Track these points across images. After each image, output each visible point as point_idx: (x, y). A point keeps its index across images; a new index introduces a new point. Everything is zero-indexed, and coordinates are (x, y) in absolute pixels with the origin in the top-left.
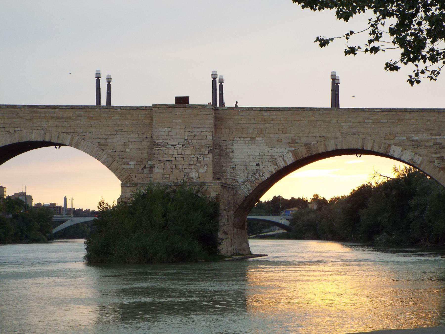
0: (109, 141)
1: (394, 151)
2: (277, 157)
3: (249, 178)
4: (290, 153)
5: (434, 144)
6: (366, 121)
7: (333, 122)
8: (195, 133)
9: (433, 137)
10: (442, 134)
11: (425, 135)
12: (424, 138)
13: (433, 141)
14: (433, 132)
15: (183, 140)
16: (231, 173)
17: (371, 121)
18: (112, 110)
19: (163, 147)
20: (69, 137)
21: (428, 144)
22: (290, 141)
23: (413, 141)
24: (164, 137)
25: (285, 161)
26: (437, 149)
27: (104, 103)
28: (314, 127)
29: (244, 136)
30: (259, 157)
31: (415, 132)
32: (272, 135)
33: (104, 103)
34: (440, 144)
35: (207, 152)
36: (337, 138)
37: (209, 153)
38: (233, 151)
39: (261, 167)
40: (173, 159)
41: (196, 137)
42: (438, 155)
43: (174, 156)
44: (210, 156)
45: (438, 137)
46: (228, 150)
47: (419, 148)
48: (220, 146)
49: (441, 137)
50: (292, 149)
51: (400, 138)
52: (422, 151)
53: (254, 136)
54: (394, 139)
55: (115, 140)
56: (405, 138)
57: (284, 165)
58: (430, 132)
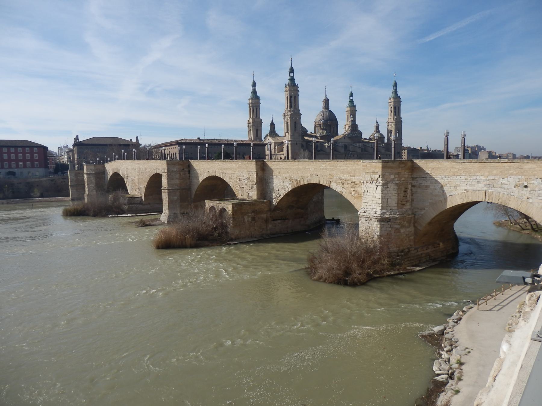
0: (232, 176)
1: (333, 186)
3: (276, 197)
4: (290, 185)
5: (352, 182)
6: (321, 167)
7: (306, 168)
8: (251, 174)
9: (351, 178)
10: (356, 176)
11: (347, 176)
15: (247, 178)
16: (270, 194)
17: (322, 167)
18: (233, 162)
19: (241, 180)
26: (353, 185)
28: (299, 171)
31: (343, 175)
32: (283, 175)
35: (254, 184)
37: (255, 184)
38: (270, 183)
39: (280, 191)
40: (244, 187)
43: (245, 185)
44: (256, 185)
45: (354, 178)
46: (268, 182)
47: (345, 184)
48: (266, 180)
50: (291, 182)
52: (346, 186)
56: (338, 178)
57: (288, 191)
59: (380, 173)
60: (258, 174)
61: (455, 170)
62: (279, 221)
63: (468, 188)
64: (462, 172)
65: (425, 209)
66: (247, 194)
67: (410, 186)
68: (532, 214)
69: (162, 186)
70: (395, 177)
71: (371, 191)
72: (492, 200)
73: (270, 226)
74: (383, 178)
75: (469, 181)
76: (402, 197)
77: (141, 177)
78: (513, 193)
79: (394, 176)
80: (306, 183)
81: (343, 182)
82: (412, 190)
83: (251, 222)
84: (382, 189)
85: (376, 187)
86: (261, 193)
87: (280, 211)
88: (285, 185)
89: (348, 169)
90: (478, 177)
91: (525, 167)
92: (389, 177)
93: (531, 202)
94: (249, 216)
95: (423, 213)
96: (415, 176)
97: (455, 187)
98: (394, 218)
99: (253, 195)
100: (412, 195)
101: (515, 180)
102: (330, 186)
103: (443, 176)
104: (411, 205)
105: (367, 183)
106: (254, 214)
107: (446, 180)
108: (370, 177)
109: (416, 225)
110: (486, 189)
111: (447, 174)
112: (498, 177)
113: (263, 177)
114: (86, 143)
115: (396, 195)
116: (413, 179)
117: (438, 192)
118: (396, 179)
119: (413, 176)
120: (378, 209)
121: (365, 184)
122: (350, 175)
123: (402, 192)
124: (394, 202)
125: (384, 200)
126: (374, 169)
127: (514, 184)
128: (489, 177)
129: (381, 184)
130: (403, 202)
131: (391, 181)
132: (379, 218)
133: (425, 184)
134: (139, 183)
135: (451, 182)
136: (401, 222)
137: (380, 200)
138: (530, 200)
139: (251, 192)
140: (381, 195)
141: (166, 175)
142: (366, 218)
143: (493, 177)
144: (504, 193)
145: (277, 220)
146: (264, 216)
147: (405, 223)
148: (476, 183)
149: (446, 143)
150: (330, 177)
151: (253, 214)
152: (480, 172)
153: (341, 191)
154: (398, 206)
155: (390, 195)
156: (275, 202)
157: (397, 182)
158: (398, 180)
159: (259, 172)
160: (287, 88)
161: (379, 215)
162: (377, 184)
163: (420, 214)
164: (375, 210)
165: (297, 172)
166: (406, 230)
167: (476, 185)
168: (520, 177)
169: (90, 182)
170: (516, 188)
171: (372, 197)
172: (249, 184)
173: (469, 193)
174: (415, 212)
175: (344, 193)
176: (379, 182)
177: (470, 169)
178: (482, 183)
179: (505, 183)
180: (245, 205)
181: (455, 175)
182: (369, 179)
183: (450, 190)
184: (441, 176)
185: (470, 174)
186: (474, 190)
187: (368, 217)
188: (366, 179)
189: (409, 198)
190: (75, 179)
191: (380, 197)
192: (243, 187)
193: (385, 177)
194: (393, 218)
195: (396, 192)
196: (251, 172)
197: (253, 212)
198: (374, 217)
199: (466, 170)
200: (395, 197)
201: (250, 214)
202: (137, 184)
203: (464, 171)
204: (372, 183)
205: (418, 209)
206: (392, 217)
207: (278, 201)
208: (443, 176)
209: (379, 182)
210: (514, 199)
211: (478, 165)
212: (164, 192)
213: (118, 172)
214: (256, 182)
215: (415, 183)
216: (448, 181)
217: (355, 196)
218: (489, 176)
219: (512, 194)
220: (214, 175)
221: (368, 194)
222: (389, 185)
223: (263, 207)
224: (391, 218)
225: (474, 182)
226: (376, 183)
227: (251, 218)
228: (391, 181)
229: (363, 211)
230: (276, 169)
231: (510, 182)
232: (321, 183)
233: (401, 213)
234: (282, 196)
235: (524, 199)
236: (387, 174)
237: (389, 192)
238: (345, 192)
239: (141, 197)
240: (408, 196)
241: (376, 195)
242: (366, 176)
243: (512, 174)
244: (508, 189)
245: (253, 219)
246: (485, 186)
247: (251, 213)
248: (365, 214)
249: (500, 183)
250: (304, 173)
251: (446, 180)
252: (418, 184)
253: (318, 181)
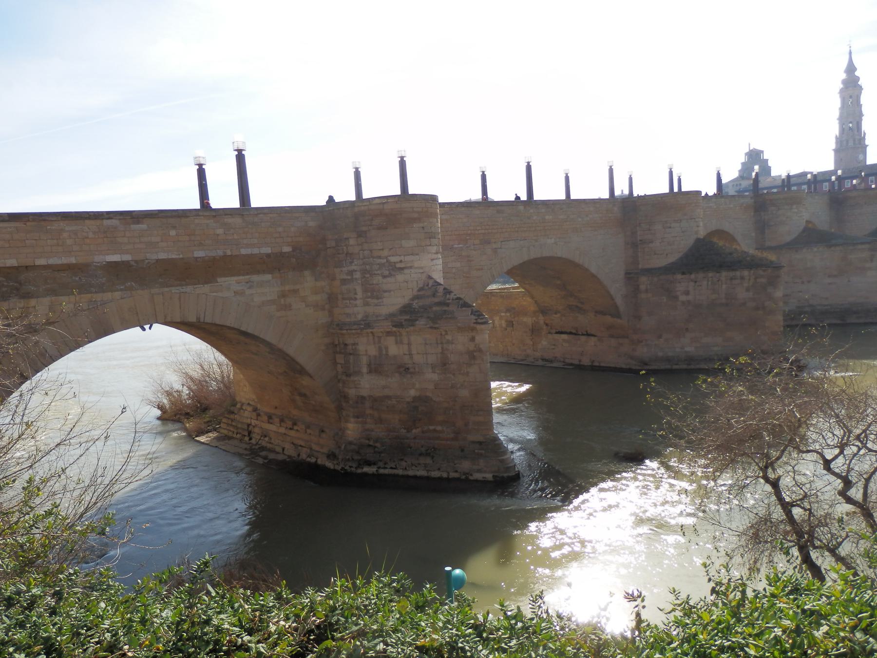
27: (676, 190)
33: (676, 190)
62: (564, 336)
73: (544, 343)
94: (501, 318)
106: (511, 315)
145: (562, 333)
146: (528, 320)
151: (508, 314)
180: (493, 296)
197: (508, 310)
201: (503, 314)
223: (525, 303)
227: (506, 321)
245: (510, 324)
247: (506, 312)
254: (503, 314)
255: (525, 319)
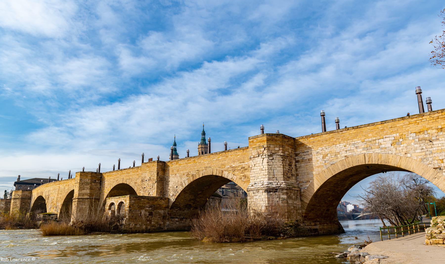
0: (137, 181)
1: (225, 174)
2: (183, 182)
5: (241, 168)
6: (214, 160)
7: (201, 162)
8: (152, 174)
9: (241, 164)
10: (245, 162)
11: (237, 163)
12: (237, 165)
13: (241, 166)
14: (241, 161)
15: (149, 178)
17: (216, 159)
20: (128, 180)
21: (239, 168)
22: (187, 174)
23: (233, 167)
24: (144, 177)
25: (185, 184)
26: (243, 171)
28: (195, 166)
29: (173, 173)
30: (177, 183)
32: (181, 172)
34: (244, 168)
35: (155, 183)
36: (203, 170)
38: (169, 181)
39: (178, 188)
40: (146, 187)
41: (152, 176)
42: (243, 174)
44: (156, 184)
45: (243, 164)
47: (235, 171)
48: (166, 179)
49: (245, 163)
50: (188, 178)
51: (227, 167)
52: (236, 173)
53: (176, 173)
54: (225, 167)
55: (138, 180)
56: (229, 166)
57: (185, 186)
58: (240, 161)
59: (265, 146)
60: (159, 174)
61: (334, 140)
63: (348, 154)
64: (341, 140)
65: (309, 182)
66: (148, 193)
67: (294, 161)
68: (413, 168)
69: (73, 197)
70: (279, 149)
71: (257, 165)
72: (372, 161)
74: (268, 150)
75: (348, 147)
76: (287, 170)
77: (59, 196)
78: (391, 151)
79: (278, 148)
80: (201, 176)
81: (234, 169)
82: (296, 165)
83: (148, 217)
84: (268, 160)
85: (262, 159)
86: (161, 192)
87: (178, 209)
88: (182, 181)
89: (238, 157)
90: (356, 142)
91: (398, 125)
92: (274, 149)
93: (409, 156)
94: (146, 211)
95: (308, 185)
96: (298, 152)
97: (335, 155)
98: (281, 189)
99: (153, 193)
100: (296, 170)
101: (390, 138)
102: (222, 175)
103: (324, 148)
104: (296, 179)
105: (253, 158)
107: (326, 151)
108: (256, 152)
109: (303, 199)
110: (365, 152)
111: (327, 145)
112: (374, 138)
113: (164, 177)
114: (27, 182)
115: (282, 166)
116: (297, 155)
117: (321, 163)
118: (281, 151)
119: (296, 153)
120: (266, 181)
121: (252, 159)
122: (240, 161)
123: (287, 165)
124: (280, 173)
125: (270, 171)
126: (259, 144)
127: (391, 142)
128: (366, 140)
129: (267, 156)
130: (288, 175)
131: (275, 153)
132: (266, 188)
133: (309, 158)
134: (57, 201)
135: (331, 151)
136: (288, 193)
137: (267, 171)
138: (409, 155)
139: (151, 191)
140: (267, 166)
141: (78, 185)
142: (254, 191)
143: (370, 139)
144: (383, 152)
147: (292, 194)
148: (355, 148)
149: (323, 122)
150: (222, 167)
151: (151, 209)
152: (357, 137)
153: (232, 178)
154: (284, 177)
155: (276, 166)
156: (173, 199)
157: (282, 154)
158: (282, 152)
159: (160, 172)
160: (200, 146)
161: (267, 186)
162: (263, 157)
163: (305, 187)
164: (262, 182)
165: (193, 168)
166: (293, 202)
167: (355, 150)
168: (395, 135)
169: (15, 206)
170: (393, 147)
171: (259, 170)
172: (150, 183)
173: (350, 158)
174: (301, 186)
175: (235, 179)
176: (265, 154)
177: (347, 137)
178: (360, 147)
179: (382, 143)
181: (334, 145)
182: (255, 153)
183: (331, 159)
184: (321, 147)
185: (348, 141)
186: (354, 155)
187: (256, 189)
188: (253, 154)
189: (294, 172)
190: (4, 207)
191: (267, 169)
192: (144, 188)
193: (270, 149)
194: (280, 188)
195: (281, 163)
196: (153, 172)
197: (151, 207)
198: (262, 188)
199: (344, 138)
200: (280, 169)
201: (147, 209)
202: (55, 203)
203: (342, 140)
204: (259, 156)
205: (303, 182)
206: (279, 187)
207: (176, 197)
208: (324, 148)
209: (265, 154)
210: (393, 157)
211: (355, 132)
212: (74, 202)
213: (42, 195)
214: (156, 180)
215: (298, 158)
216: (328, 151)
217: (245, 180)
218: (365, 140)
219: (390, 152)
220: (122, 183)
221: (255, 168)
222: (274, 156)
224: (277, 188)
225: (353, 147)
226: (262, 155)
227: (149, 212)
228: (275, 153)
229: (251, 185)
230: (176, 168)
231: (386, 142)
232: (214, 174)
233: (287, 184)
234: (180, 192)
235: (402, 155)
236: (271, 146)
237: (274, 164)
238: (236, 178)
239: (57, 215)
240: (293, 170)
241: (262, 167)
242: (252, 151)
243: (386, 134)
244: (386, 148)
245: (151, 214)
246: (364, 149)
247: (149, 208)
248: (253, 187)
249: (377, 144)
250: (199, 167)
251: (326, 151)
252: (301, 159)
253: (212, 172)
254: (147, 209)
255: (160, 211)
